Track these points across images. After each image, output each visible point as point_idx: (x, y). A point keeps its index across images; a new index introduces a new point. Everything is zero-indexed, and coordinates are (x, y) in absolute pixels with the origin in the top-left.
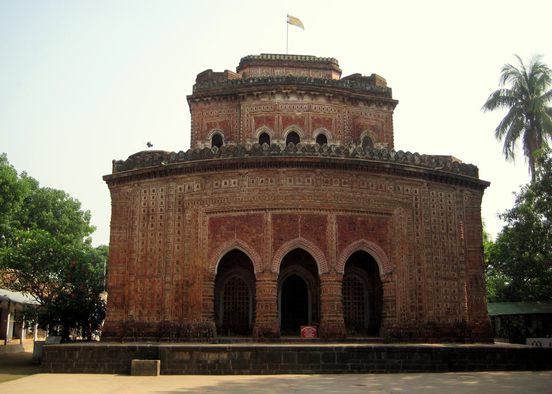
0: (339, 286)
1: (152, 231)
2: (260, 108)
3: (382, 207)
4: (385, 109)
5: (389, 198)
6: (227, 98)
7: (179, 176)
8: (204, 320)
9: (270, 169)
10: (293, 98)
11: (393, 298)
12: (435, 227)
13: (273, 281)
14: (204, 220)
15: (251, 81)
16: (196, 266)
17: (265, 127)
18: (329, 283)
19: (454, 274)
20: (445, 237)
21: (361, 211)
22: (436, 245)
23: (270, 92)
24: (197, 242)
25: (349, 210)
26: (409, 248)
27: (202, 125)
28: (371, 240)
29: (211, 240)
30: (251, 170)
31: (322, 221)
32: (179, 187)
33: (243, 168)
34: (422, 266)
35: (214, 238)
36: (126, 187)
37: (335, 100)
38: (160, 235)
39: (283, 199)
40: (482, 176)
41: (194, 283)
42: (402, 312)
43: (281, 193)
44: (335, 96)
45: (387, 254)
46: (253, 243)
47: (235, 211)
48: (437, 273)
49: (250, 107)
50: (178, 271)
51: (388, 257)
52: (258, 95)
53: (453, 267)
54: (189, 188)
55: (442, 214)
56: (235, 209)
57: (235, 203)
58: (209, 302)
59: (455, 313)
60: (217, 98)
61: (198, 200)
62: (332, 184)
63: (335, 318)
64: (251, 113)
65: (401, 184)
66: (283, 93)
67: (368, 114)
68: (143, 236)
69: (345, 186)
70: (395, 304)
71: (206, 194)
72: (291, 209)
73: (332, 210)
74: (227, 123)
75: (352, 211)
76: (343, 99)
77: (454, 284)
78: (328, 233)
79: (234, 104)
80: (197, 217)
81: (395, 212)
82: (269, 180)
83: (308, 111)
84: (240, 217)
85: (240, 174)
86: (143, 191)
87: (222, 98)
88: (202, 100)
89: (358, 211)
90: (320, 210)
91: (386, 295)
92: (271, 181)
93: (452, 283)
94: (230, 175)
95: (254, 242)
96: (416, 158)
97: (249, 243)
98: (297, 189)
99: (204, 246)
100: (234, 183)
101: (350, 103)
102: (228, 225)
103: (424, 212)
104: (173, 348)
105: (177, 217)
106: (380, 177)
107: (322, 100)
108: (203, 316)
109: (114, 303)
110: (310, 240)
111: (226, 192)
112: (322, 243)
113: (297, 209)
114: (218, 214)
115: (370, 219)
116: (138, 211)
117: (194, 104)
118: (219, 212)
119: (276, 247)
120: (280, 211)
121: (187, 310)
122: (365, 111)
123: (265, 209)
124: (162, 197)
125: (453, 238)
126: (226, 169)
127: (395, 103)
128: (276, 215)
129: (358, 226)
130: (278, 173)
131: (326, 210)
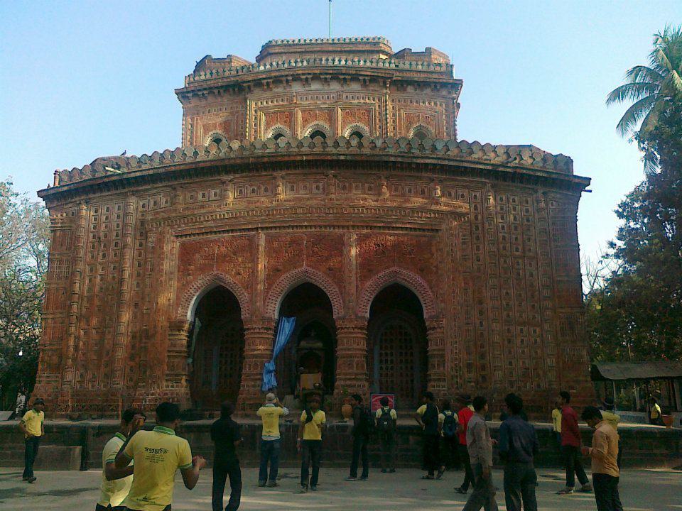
0: (361, 335)
4: (444, 93)
6: (229, 91)
7: (141, 188)
8: (167, 386)
10: (315, 86)
12: (504, 248)
13: (266, 329)
14: (172, 247)
18: (346, 330)
19: (534, 317)
20: (520, 261)
22: (506, 273)
23: (284, 79)
26: (464, 279)
29: (181, 273)
31: (338, 246)
32: (141, 203)
33: (228, 173)
37: (372, 84)
39: (280, 214)
40: (579, 170)
41: (156, 333)
42: (453, 373)
43: (278, 206)
44: (374, 79)
45: (431, 288)
47: (215, 232)
48: (508, 316)
51: (433, 292)
52: (268, 84)
53: (533, 306)
54: (155, 203)
55: (516, 228)
58: (176, 360)
59: (538, 375)
60: (216, 91)
62: (350, 191)
63: (354, 382)
65: (453, 187)
66: (301, 80)
68: (91, 270)
69: (370, 192)
72: (293, 227)
73: (350, 228)
74: (230, 124)
77: (535, 331)
81: (443, 227)
82: (263, 188)
85: (223, 183)
90: (334, 228)
91: (432, 348)
92: (266, 190)
93: (532, 329)
94: (208, 183)
98: (300, 199)
104: (100, 427)
106: (421, 178)
107: (355, 86)
109: (49, 365)
111: (202, 207)
113: (301, 227)
120: (278, 231)
121: (145, 372)
124: (118, 217)
127: (456, 85)
130: (275, 178)
131: (343, 227)
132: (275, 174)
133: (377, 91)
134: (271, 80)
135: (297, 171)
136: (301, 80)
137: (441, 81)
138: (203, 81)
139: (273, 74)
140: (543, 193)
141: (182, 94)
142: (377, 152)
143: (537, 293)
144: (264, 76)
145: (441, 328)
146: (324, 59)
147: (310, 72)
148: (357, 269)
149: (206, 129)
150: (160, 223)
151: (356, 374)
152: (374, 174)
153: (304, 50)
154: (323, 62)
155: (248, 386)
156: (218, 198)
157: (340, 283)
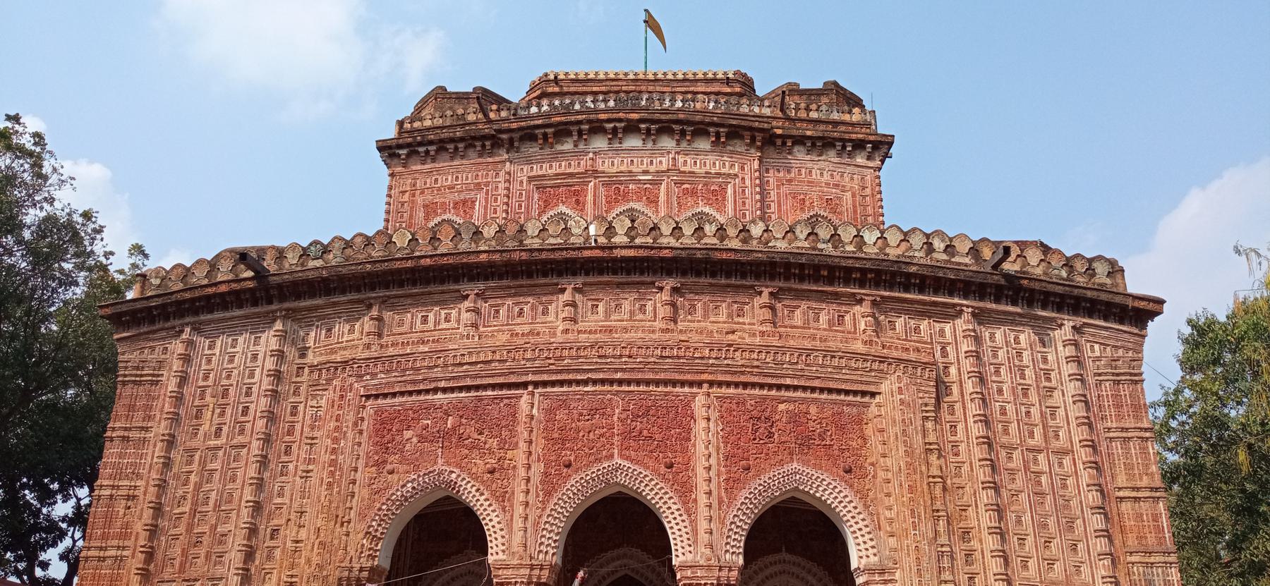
1: (218, 448)
3: (845, 374)
4: (860, 160)
7: (303, 304)
9: (543, 281)
12: (1006, 432)
20: (1041, 457)
21: (788, 387)
23: (575, 128)
25: (753, 385)
28: (817, 467)
30: (492, 284)
31: (682, 419)
34: (975, 544)
35: (380, 464)
39: (571, 358)
45: (866, 507)
47: (444, 390)
52: (545, 135)
56: (443, 384)
64: (531, 179)
67: (817, 171)
69: (741, 320)
72: (595, 382)
74: (473, 202)
75: (762, 386)
76: (753, 139)
78: (700, 448)
79: (490, 160)
81: (885, 387)
82: (541, 308)
84: (459, 408)
87: (461, 145)
89: (779, 387)
90: (674, 383)
94: (436, 297)
96: (938, 245)
98: (610, 330)
101: (772, 148)
106: (836, 296)
114: (398, 400)
115: (813, 410)
117: (396, 161)
118: (402, 394)
119: (549, 487)
122: (810, 165)
123: (524, 385)
126: (428, 282)
130: (563, 291)
131: (691, 384)
132: (563, 281)
133: (740, 153)
135: (605, 278)
136: (604, 131)
137: (854, 136)
138: (428, 129)
140: (1074, 327)
141: (387, 150)
143: (1079, 522)
144: (540, 122)
147: (621, 115)
148: (719, 464)
150: (336, 369)
154: (643, 103)
156: (453, 324)
157: (685, 491)
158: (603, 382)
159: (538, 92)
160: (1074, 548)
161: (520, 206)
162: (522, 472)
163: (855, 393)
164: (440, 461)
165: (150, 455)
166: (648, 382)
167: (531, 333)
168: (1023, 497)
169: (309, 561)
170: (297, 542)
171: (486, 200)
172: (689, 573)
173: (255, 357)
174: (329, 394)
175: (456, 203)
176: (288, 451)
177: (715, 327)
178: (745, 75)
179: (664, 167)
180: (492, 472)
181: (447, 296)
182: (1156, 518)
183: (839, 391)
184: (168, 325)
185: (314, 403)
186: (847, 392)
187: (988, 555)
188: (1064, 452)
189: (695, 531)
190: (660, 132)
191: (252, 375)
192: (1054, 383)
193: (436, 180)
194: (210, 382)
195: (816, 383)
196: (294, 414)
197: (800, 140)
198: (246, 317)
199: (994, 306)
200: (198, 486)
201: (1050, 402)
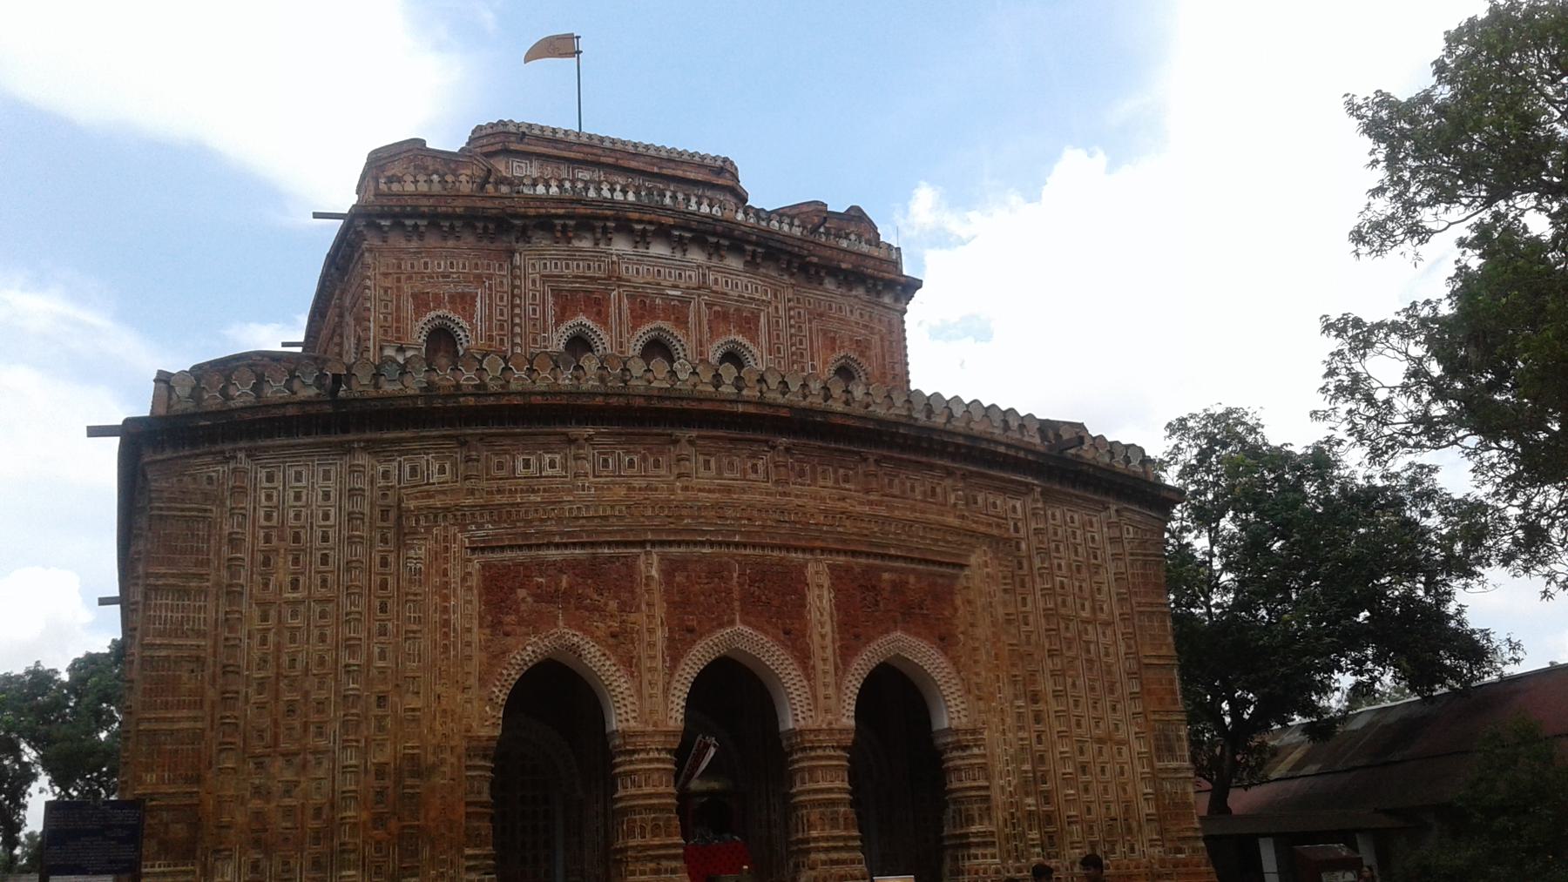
1: (296, 602)
2: (567, 267)
5: (957, 522)
9: (655, 431)
10: (658, 249)
11: (983, 793)
12: (1064, 602)
15: (541, 190)
16: (445, 711)
17: (582, 319)
18: (820, 752)
20: (1090, 628)
21: (891, 557)
22: (1069, 648)
24: (446, 635)
27: (398, 297)
28: (918, 634)
29: (488, 631)
32: (381, 469)
33: (579, 423)
34: (1041, 706)
35: (496, 625)
36: (208, 459)
38: (323, 615)
46: (611, 641)
47: (557, 546)
49: (540, 261)
50: (381, 728)
52: (564, 226)
54: (413, 470)
56: (557, 539)
57: (560, 519)
59: (1129, 830)
61: (446, 509)
62: (814, 480)
63: (845, 855)
68: (265, 618)
70: (988, 809)
71: (472, 492)
72: (712, 544)
74: (474, 298)
75: (868, 555)
76: (789, 263)
77: (1120, 753)
78: (814, 616)
79: (492, 247)
80: (446, 560)
83: (699, 288)
84: (571, 565)
85: (572, 441)
86: (262, 474)
87: (458, 224)
88: (398, 224)
89: (883, 556)
90: (788, 549)
95: (614, 636)
96: (1014, 424)
97: (598, 641)
98: (728, 490)
99: (467, 651)
100: (552, 465)
102: (539, 586)
103: (1037, 563)
105: (378, 560)
106: (931, 467)
107: (734, 263)
108: (469, 869)
110: (766, 633)
112: (796, 641)
113: (728, 545)
114: (508, 554)
115: (912, 579)
116: (249, 538)
118: (511, 547)
119: (675, 654)
120: (683, 549)
122: (840, 300)
123: (642, 544)
124: (327, 496)
125: (1109, 632)
128: (672, 562)
129: (886, 594)
130: (676, 442)
131: (804, 550)
132: (677, 433)
134: (572, 223)
135: (720, 433)
136: (631, 232)
139: (581, 210)
142: (857, 409)
144: (561, 211)
145: (978, 746)
146: (668, 194)
149: (422, 302)
150: (436, 516)
151: (845, 838)
152: (859, 453)
153: (580, 156)
154: (667, 201)
155: (643, 873)
156: (558, 471)
157: (804, 659)
158: (720, 544)
159: (499, 147)
160: (1114, 709)
161: (534, 311)
162: (646, 636)
163: (948, 564)
164: (561, 624)
165: (211, 605)
166: (763, 547)
167: (648, 488)
168: (1078, 663)
169: (431, 730)
170: (413, 710)
171: (490, 296)
172: (812, 737)
173: (327, 496)
174: (431, 544)
175: (452, 297)
176: (383, 609)
177: (825, 493)
178: (732, 163)
179: (694, 282)
180: (614, 636)
181: (552, 438)
182: (1171, 682)
183: (934, 563)
184: (218, 448)
185: (412, 553)
186: (941, 564)
187: (1052, 715)
188: (1107, 624)
189: (815, 697)
190: (692, 240)
191: (326, 517)
192: (1099, 561)
193: (426, 264)
194: (274, 522)
195: (916, 555)
196: (384, 563)
197: (834, 272)
198: (316, 445)
199: (1057, 487)
200: (278, 647)
201: (1097, 578)
